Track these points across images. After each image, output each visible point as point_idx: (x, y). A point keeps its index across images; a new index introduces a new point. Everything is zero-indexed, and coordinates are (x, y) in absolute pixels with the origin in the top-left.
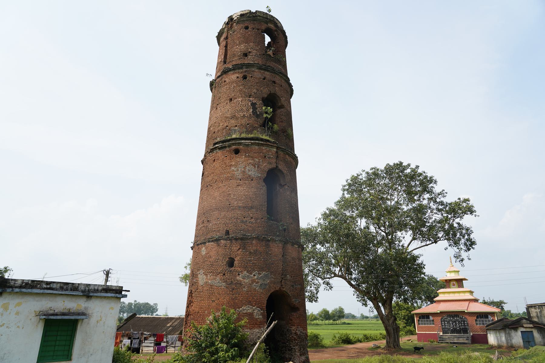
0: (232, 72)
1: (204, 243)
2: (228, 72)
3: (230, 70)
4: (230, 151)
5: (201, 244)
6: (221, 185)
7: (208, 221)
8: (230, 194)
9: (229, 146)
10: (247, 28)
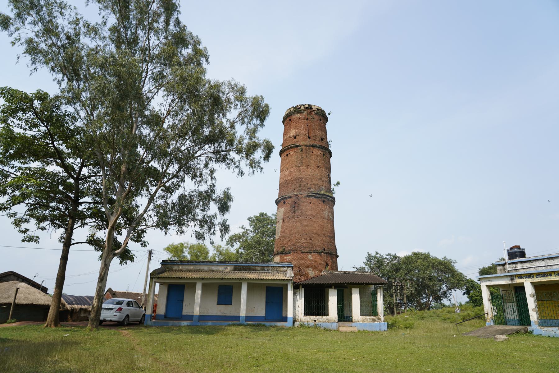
0: (317, 148)
1: (310, 253)
2: (315, 147)
3: (317, 147)
4: (321, 200)
5: (307, 253)
6: (318, 220)
7: (311, 240)
8: (323, 227)
9: (321, 198)
10: (320, 120)
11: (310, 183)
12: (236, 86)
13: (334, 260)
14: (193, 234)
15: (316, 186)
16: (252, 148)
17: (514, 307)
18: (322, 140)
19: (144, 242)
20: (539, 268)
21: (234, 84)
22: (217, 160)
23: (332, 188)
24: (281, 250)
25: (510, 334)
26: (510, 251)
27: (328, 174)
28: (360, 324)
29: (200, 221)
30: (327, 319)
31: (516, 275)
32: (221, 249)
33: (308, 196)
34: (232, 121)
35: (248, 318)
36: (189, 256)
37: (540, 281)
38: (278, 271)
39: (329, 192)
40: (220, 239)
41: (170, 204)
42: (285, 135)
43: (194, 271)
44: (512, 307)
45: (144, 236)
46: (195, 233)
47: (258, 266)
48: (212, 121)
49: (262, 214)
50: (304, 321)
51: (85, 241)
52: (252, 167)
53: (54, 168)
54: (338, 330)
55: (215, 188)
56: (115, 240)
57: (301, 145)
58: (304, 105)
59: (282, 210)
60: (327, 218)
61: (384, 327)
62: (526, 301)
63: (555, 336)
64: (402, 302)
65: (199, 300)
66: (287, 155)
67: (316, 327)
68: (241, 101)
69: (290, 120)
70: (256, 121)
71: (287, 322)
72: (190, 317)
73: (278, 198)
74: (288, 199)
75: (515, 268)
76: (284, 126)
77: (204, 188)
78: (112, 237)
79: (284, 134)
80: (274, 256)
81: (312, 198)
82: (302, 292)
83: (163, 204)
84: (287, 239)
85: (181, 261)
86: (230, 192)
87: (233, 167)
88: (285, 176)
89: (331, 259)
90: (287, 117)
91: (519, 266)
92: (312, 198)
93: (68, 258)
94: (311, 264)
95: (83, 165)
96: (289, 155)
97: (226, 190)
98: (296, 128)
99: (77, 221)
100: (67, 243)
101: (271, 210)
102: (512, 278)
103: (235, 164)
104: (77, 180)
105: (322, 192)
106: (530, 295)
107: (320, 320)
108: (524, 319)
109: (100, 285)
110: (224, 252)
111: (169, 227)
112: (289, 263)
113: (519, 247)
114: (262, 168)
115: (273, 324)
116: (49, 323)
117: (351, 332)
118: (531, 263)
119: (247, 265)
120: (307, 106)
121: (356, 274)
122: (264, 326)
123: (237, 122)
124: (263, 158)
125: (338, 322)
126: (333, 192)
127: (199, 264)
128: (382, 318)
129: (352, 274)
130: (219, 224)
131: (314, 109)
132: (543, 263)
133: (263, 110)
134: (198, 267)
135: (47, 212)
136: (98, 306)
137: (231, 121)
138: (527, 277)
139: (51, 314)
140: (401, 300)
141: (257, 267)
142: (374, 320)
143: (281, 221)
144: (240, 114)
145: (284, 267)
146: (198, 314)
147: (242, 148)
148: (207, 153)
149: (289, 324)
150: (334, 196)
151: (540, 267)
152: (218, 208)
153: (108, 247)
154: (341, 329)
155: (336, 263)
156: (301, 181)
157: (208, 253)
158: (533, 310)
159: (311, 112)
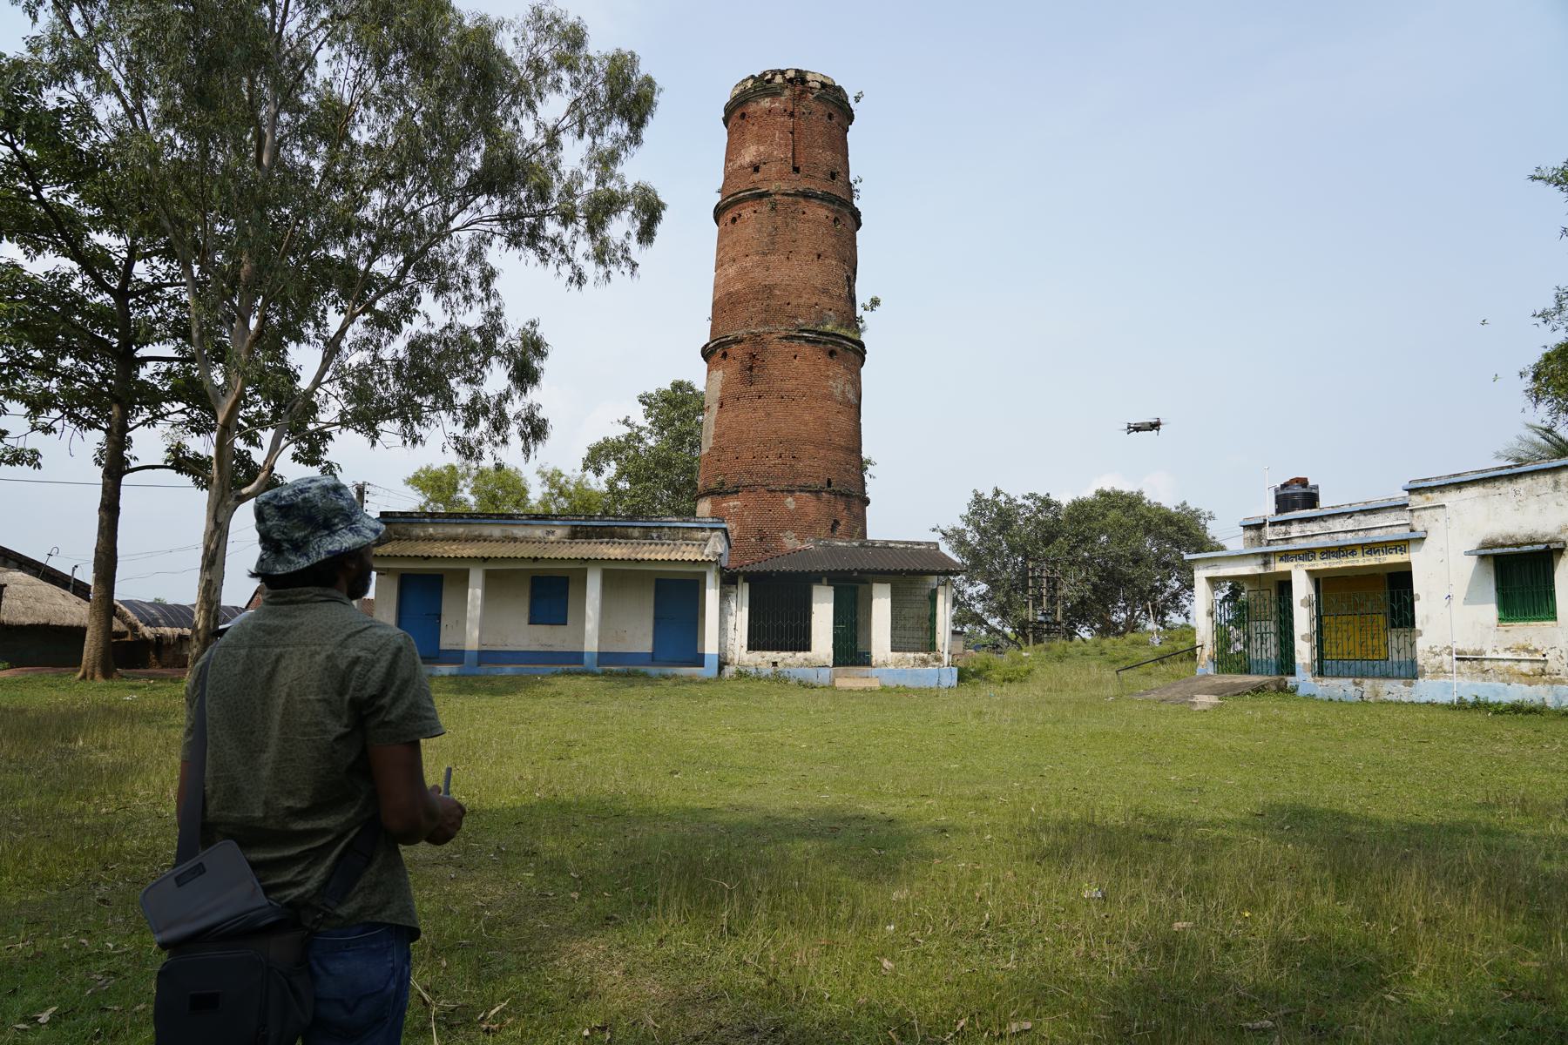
0: (818, 202)
2: (811, 197)
3: (817, 197)
5: (782, 491)
8: (829, 424)
9: (825, 343)
10: (830, 116)
11: (794, 302)
12: (557, 21)
13: (856, 510)
14: (446, 444)
15: (812, 310)
16: (603, 208)
17: (1263, 631)
18: (833, 176)
19: (330, 465)
20: (1340, 535)
21: (552, 16)
22: (514, 240)
23: (858, 315)
24: (713, 485)
25: (1239, 694)
26: (1282, 492)
27: (848, 278)
28: (889, 671)
29: (466, 409)
30: (806, 659)
31: (1275, 553)
32: (563, 480)
33: (789, 338)
34: (550, 126)
35: (604, 657)
36: (472, 500)
37: (1327, 567)
38: (686, 539)
39: (848, 327)
40: (522, 456)
41: (388, 363)
42: (730, 161)
43: (466, 541)
44: (1258, 631)
45: (326, 450)
46: (453, 441)
47: (635, 527)
48: (489, 127)
49: (678, 386)
50: (746, 663)
51: (162, 464)
52: (603, 262)
53: (46, 264)
54: (832, 686)
55: (502, 321)
56: (244, 460)
57: (771, 192)
58: (783, 73)
59: (719, 375)
60: (840, 399)
61: (950, 678)
62: (1291, 616)
63: (1344, 699)
64: (1049, 619)
65: (478, 612)
66: (734, 220)
67: (779, 679)
68: (571, 68)
69: (743, 116)
70: (619, 128)
71: (703, 666)
72: (456, 656)
73: (708, 341)
74: (734, 347)
75: (1285, 534)
76: (726, 131)
77: (472, 318)
78: (227, 452)
79: (728, 160)
80: (696, 499)
81: (800, 345)
82: (744, 592)
83: (369, 362)
84: (730, 455)
85: (450, 516)
86: (539, 331)
87: (557, 262)
88: (727, 282)
89: (848, 508)
90: (735, 109)
91: (1295, 530)
92: (800, 345)
93: (119, 508)
94: (793, 521)
95: (134, 254)
96: (738, 221)
97: (528, 327)
98: (760, 140)
99: (138, 409)
100: (115, 466)
101: (697, 374)
102: (1267, 559)
103: (562, 250)
104: (121, 295)
105: (829, 327)
106: (1302, 601)
107: (789, 661)
108: (1286, 663)
109: (208, 576)
110: (572, 488)
111: (381, 426)
112: (715, 520)
113: (1303, 482)
114: (635, 265)
115: (669, 671)
116: (89, 671)
117: (864, 690)
118: (1322, 524)
119: (606, 524)
120: (791, 74)
121: (891, 548)
122: (646, 676)
123: (564, 129)
124: (634, 237)
125: (834, 665)
126: (861, 326)
127: (478, 521)
128: (946, 658)
129: (880, 547)
130: (517, 416)
131: (811, 84)
132: (1349, 524)
133: (637, 96)
134: (476, 530)
135: (54, 383)
136: (207, 627)
137: (550, 126)
138: (1300, 559)
139: (91, 647)
140: (1049, 614)
141: (630, 530)
142: (925, 662)
143: (715, 407)
144: (575, 104)
145: (702, 528)
146: (476, 648)
147: (575, 208)
148: (481, 220)
149: (710, 670)
150: (864, 338)
151: (1341, 531)
152: (510, 376)
153: (220, 478)
154: (839, 683)
155: (861, 520)
156: (771, 296)
157: (524, 491)
158: (1303, 637)
159: (803, 92)
